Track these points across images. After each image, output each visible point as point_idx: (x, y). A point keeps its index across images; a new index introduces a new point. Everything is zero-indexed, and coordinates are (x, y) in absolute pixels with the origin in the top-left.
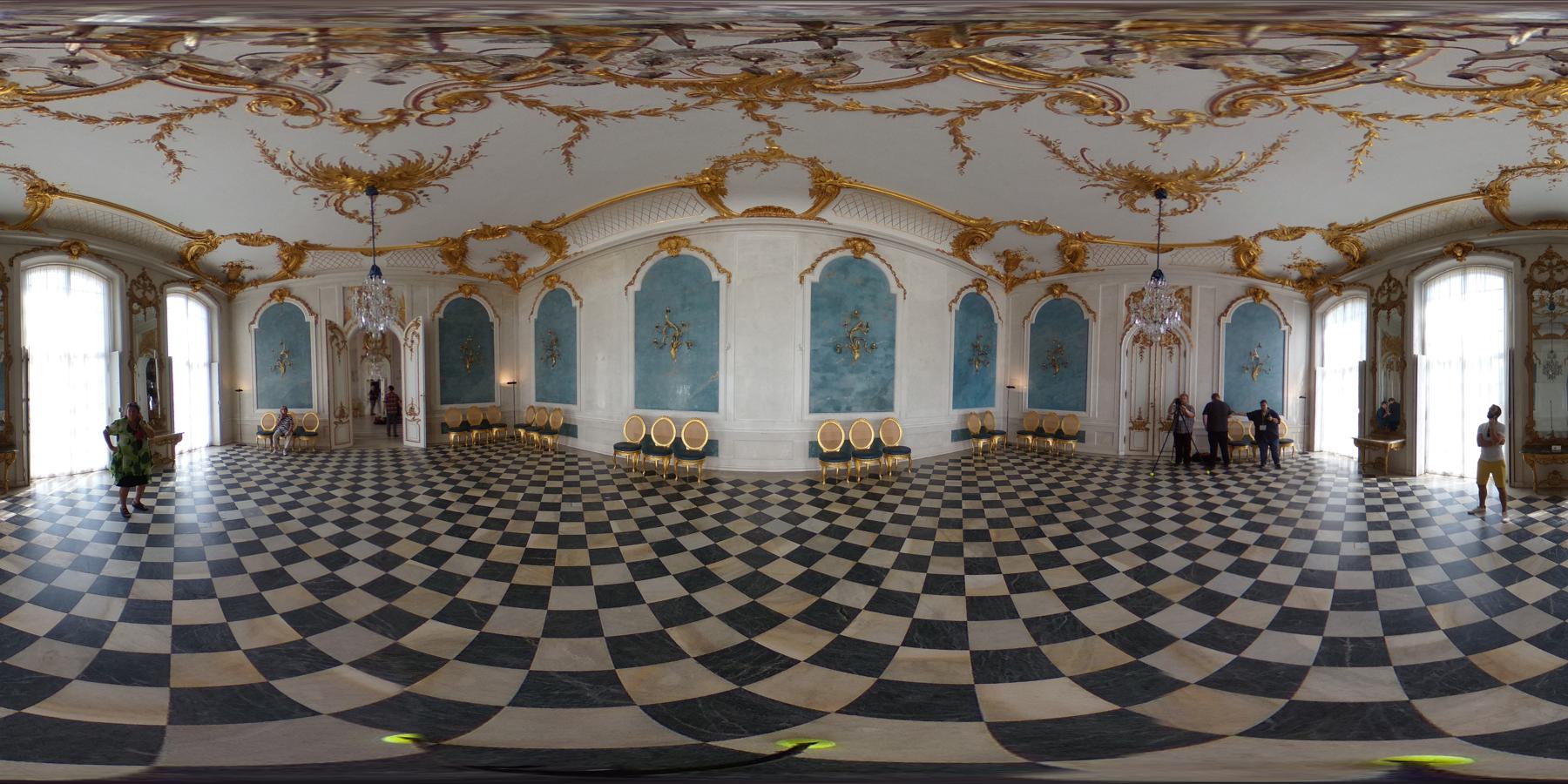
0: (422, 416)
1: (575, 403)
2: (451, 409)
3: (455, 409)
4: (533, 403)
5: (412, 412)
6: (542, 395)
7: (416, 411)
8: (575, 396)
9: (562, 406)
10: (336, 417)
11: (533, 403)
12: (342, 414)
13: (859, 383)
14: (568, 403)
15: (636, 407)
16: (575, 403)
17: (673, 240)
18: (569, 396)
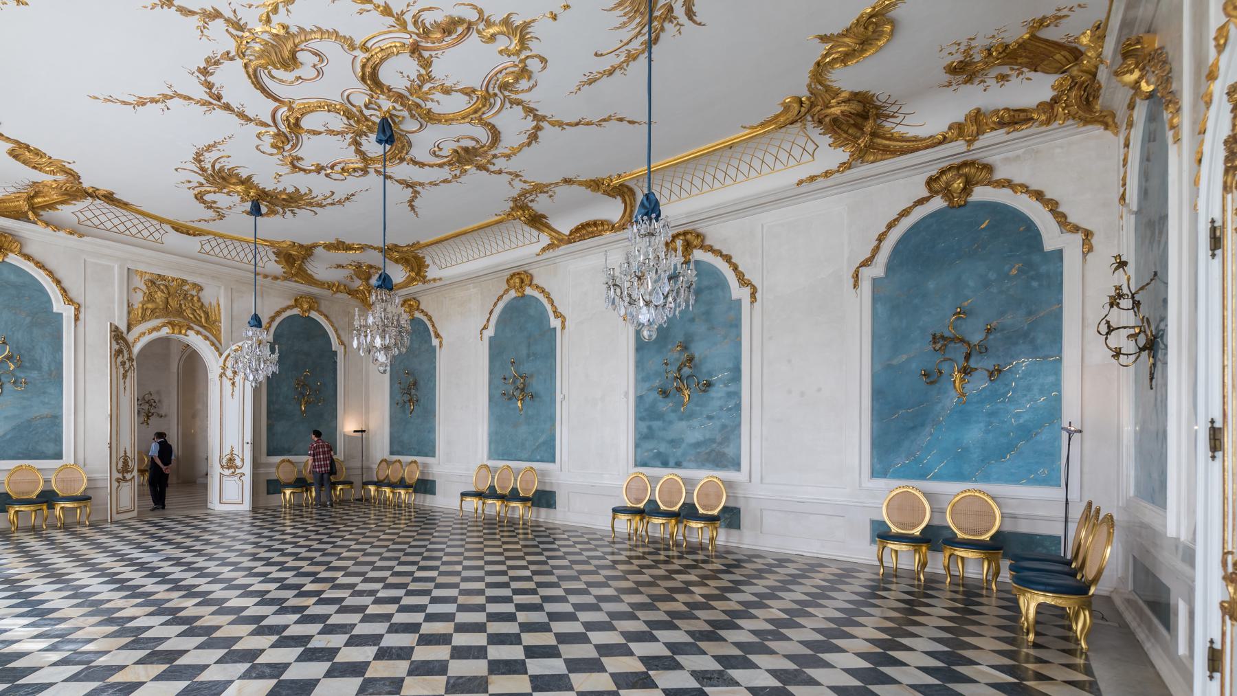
0: (247, 469)
1: (434, 456)
2: (283, 461)
3: (289, 461)
4: (386, 455)
5: (231, 464)
6: (397, 446)
7: (238, 462)
8: (434, 447)
9: (419, 459)
10: (118, 471)
11: (386, 455)
12: (125, 469)
13: (693, 433)
14: (426, 455)
15: (490, 458)
16: (434, 456)
17: (520, 278)
18: (427, 448)
